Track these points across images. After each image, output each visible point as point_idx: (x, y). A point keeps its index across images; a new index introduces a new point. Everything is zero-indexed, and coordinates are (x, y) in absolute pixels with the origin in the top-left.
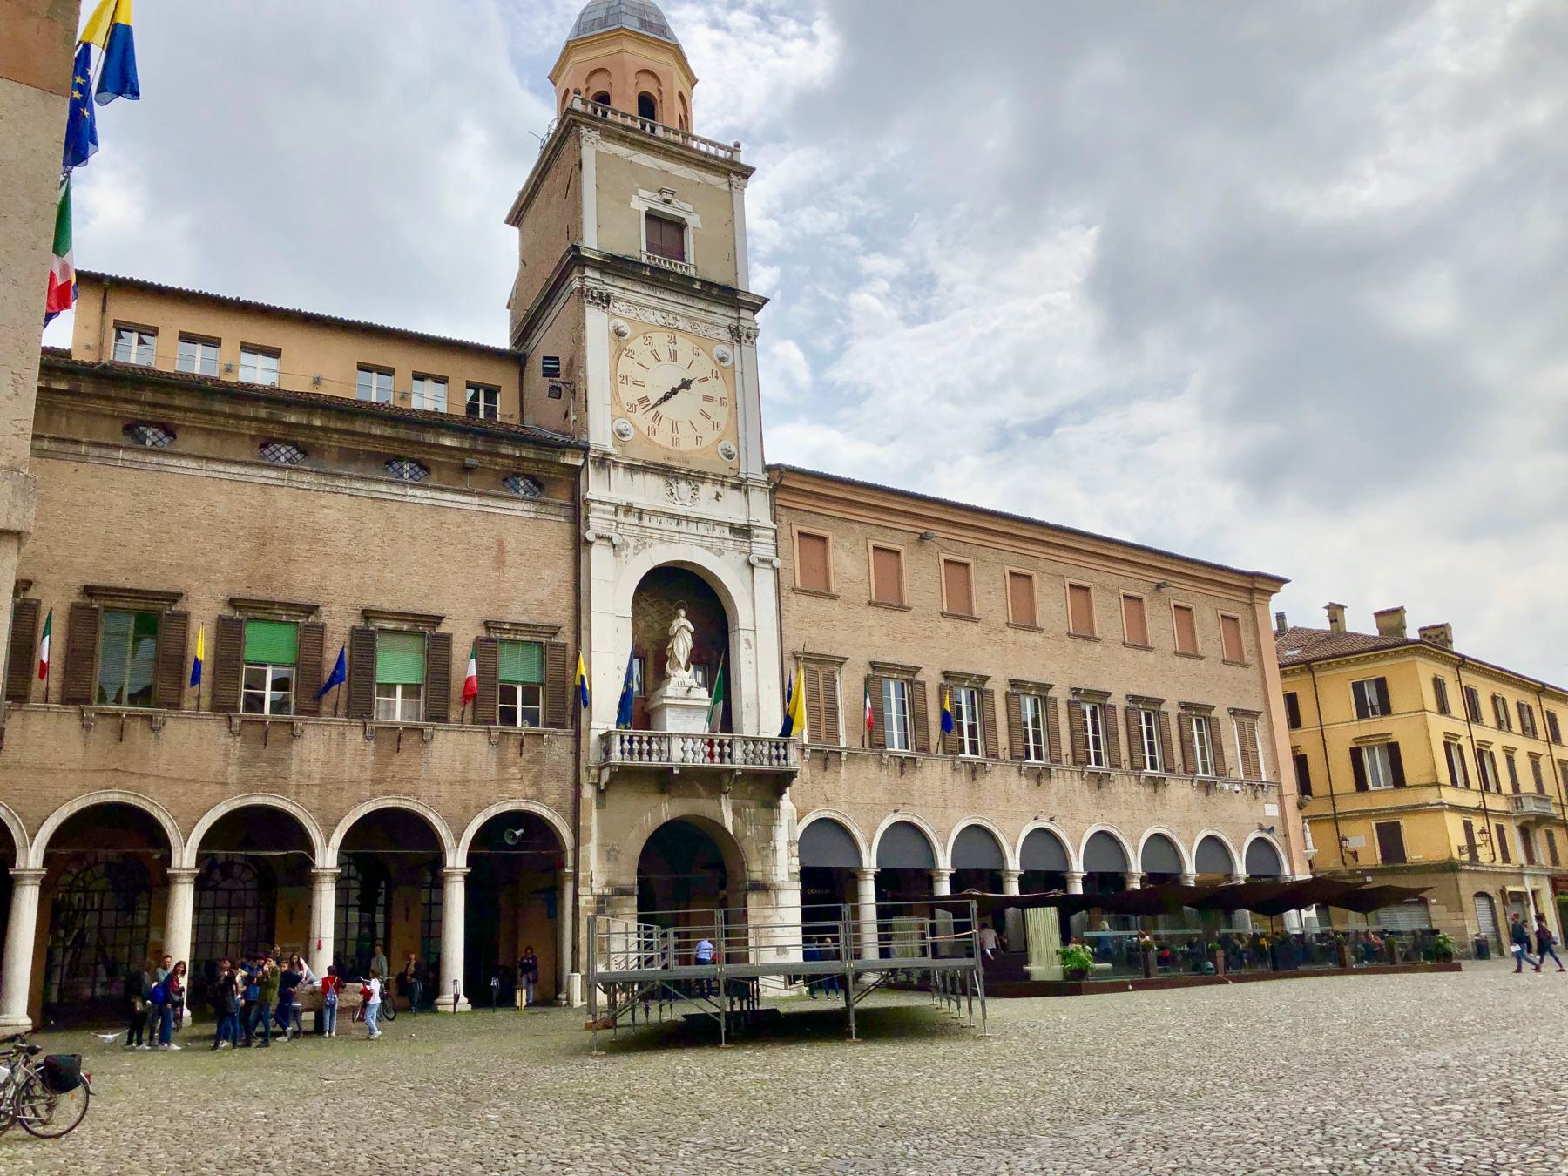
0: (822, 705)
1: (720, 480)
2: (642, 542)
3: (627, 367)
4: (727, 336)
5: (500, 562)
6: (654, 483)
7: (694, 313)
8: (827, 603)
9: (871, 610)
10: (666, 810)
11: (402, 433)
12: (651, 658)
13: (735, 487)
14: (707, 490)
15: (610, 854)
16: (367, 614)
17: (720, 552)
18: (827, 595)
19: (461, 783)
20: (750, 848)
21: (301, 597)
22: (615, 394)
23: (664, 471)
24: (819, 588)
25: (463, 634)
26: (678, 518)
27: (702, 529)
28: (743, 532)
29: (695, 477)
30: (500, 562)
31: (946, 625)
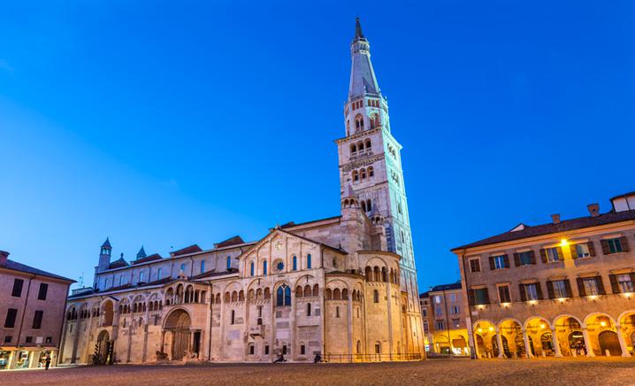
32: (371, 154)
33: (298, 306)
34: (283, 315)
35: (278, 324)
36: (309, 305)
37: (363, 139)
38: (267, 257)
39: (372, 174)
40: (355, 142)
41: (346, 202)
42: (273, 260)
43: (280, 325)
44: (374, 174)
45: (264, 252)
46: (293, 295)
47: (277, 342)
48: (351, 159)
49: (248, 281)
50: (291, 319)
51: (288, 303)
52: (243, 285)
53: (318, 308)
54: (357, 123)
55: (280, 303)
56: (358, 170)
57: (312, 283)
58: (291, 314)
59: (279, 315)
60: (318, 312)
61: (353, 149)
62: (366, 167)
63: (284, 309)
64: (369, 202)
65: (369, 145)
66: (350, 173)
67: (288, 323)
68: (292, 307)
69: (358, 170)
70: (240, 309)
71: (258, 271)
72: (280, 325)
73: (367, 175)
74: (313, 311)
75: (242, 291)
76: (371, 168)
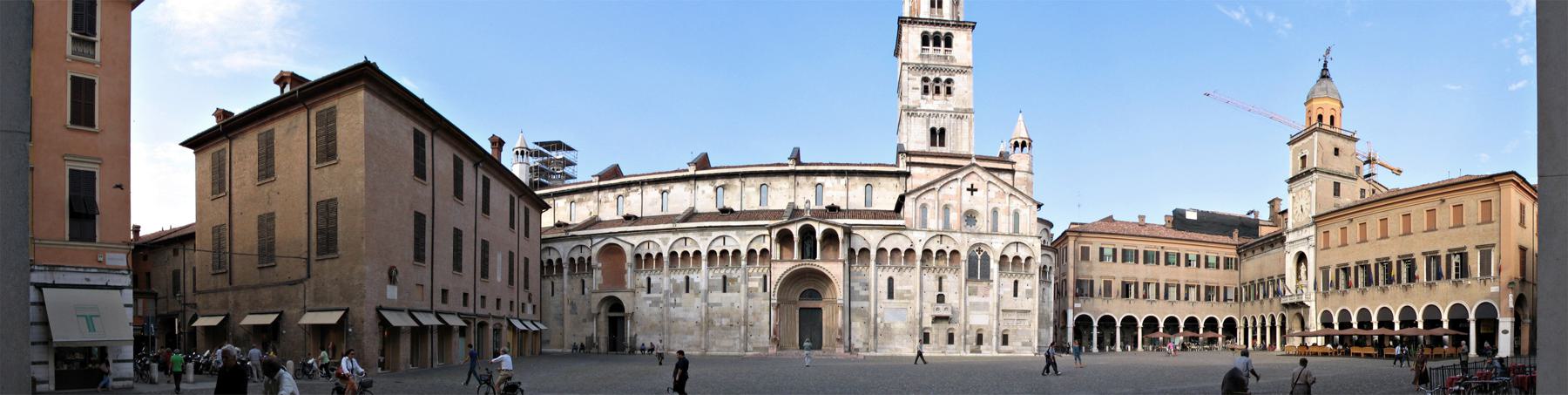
32: (952, 59)
33: (1000, 283)
37: (943, 31)
39: (949, 91)
40: (931, 30)
44: (954, 92)
46: (994, 266)
49: (924, 236)
50: (992, 299)
52: (918, 239)
55: (972, 275)
56: (932, 78)
58: (993, 292)
60: (1029, 293)
61: (925, 40)
62: (944, 78)
64: (943, 131)
65: (949, 44)
68: (995, 284)
69: (932, 78)
71: (934, 223)
72: (976, 306)
73: (943, 90)
75: (910, 251)
76: (949, 81)
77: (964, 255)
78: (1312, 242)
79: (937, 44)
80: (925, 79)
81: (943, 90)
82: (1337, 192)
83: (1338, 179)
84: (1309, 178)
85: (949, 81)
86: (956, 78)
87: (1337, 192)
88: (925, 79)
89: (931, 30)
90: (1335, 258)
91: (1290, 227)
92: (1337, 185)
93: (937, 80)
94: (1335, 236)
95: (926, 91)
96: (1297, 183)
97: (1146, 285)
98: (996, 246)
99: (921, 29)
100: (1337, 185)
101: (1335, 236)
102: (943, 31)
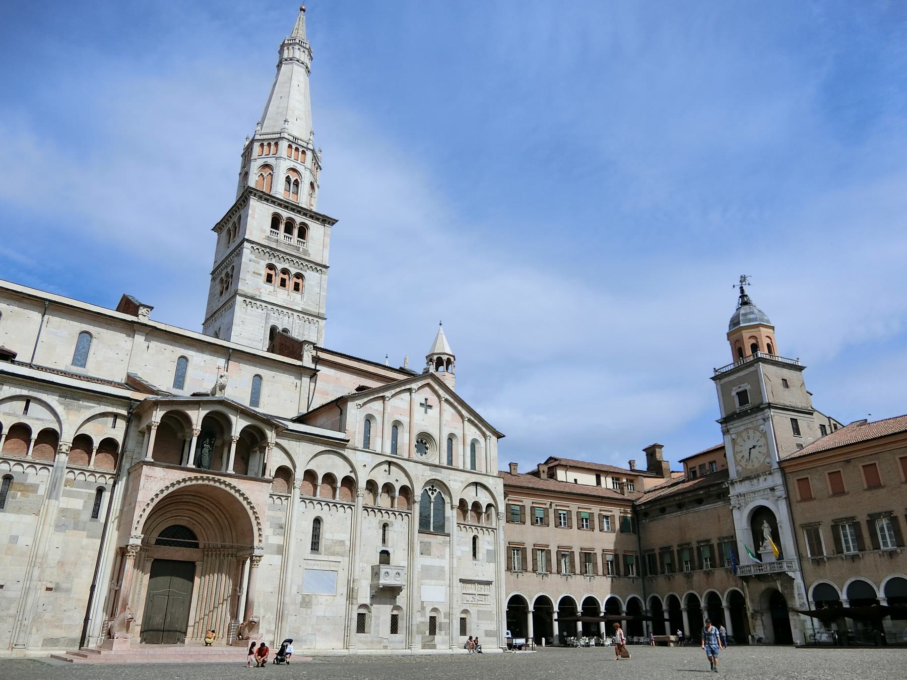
0: (814, 542)
1: (764, 473)
2: (746, 504)
3: (738, 449)
4: (761, 421)
5: (719, 520)
6: (747, 482)
7: (752, 420)
8: (812, 503)
9: (831, 499)
10: (763, 586)
11: (693, 493)
12: (758, 538)
13: (770, 474)
14: (762, 479)
15: (752, 601)
16: (698, 542)
17: (768, 499)
18: (810, 499)
19: (722, 584)
20: (787, 597)
21: (688, 541)
22: (735, 458)
23: (748, 478)
24: (807, 497)
25: (715, 542)
26: (754, 492)
27: (762, 493)
28: (772, 489)
29: (757, 477)
30: (719, 520)
31: (868, 494)
32: (306, 252)
34: (434, 550)
35: (426, 570)
36: (475, 539)
38: (405, 420)
39: (297, 287)
40: (285, 214)
41: (449, 362)
42: (415, 432)
43: (427, 572)
45: (398, 405)
47: (423, 608)
48: (268, 238)
51: (440, 529)
53: (491, 548)
54: (288, 179)
55: (424, 526)
56: (280, 266)
57: (484, 499)
59: (426, 550)
61: (275, 221)
62: (293, 271)
63: (436, 540)
65: (302, 233)
66: (264, 263)
67: (442, 569)
69: (280, 266)
70: (337, 524)
73: (290, 284)
74: (481, 554)
77: (418, 492)
78: (781, 491)
79: (289, 229)
80: (271, 267)
81: (290, 284)
82: (797, 431)
83: (795, 415)
84: (760, 416)
85: (299, 276)
86: (309, 274)
87: (797, 431)
88: (271, 267)
89: (285, 214)
90: (826, 510)
91: (733, 474)
92: (794, 421)
93: (285, 271)
94: (819, 483)
95: (269, 279)
96: (737, 423)
97: (871, 522)
98: (457, 483)
99: (272, 209)
100: (794, 421)
101: (819, 483)
102: (299, 219)
